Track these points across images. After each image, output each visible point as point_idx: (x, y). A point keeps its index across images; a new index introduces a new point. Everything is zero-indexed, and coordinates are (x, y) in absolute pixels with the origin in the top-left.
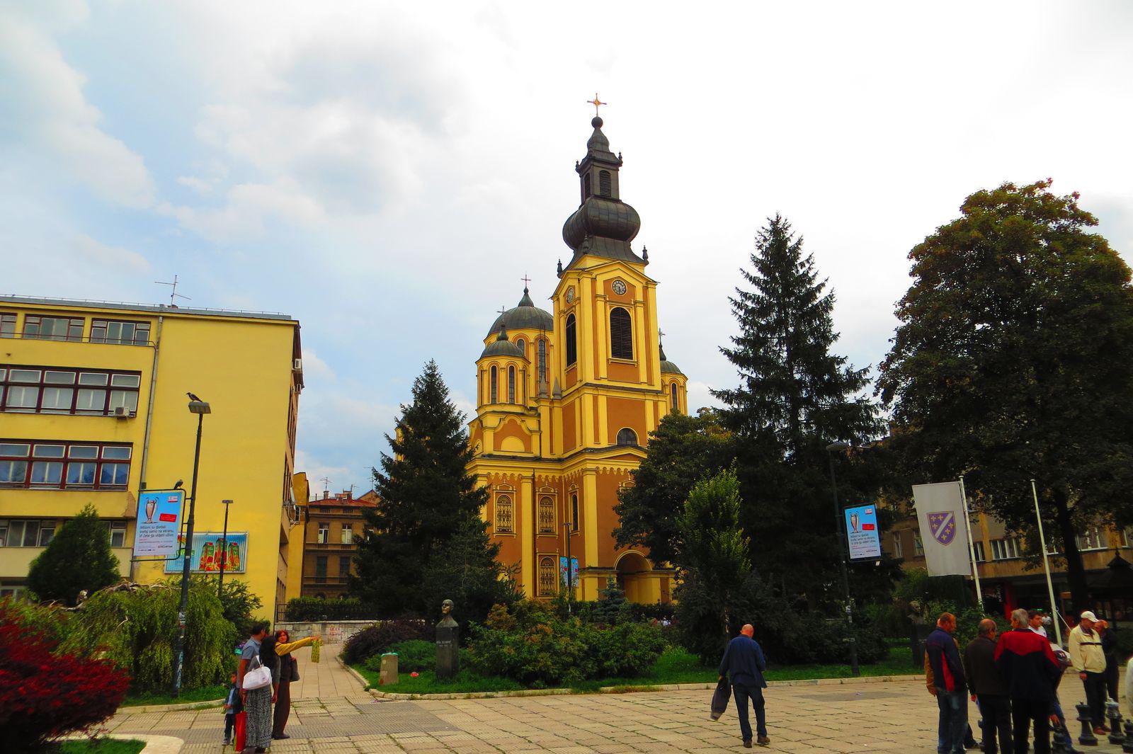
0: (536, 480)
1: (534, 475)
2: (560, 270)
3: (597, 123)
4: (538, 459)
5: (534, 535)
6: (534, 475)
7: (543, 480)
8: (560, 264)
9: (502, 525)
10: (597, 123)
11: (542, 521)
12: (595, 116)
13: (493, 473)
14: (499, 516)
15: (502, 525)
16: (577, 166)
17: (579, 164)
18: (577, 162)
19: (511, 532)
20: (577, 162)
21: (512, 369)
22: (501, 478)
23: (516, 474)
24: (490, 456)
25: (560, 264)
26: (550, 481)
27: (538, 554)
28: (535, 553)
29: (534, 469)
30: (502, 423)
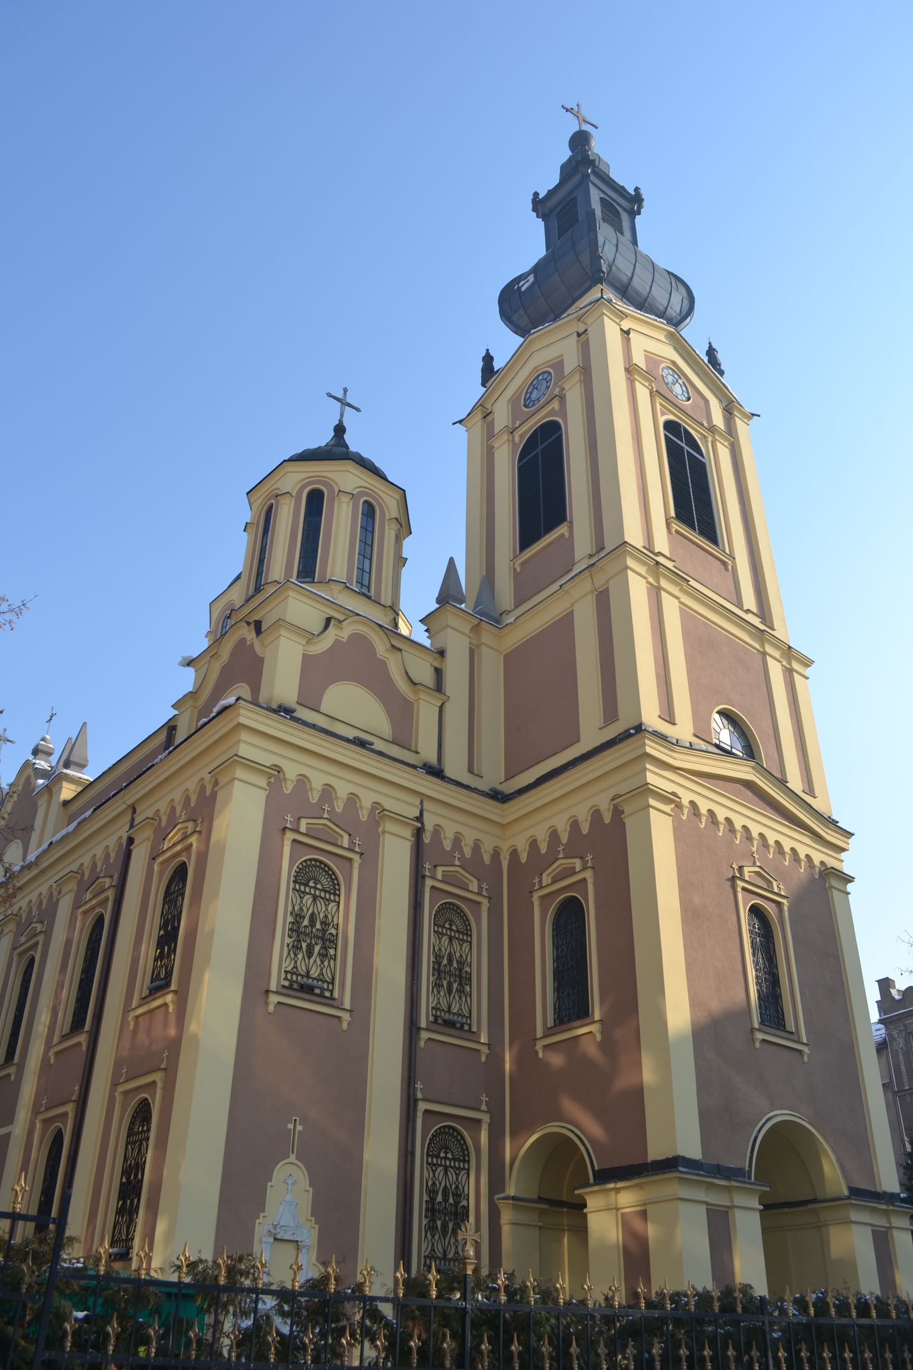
0: (427, 838)
1: (420, 819)
4: (436, 772)
5: (412, 1028)
6: (420, 819)
7: (448, 845)
8: (488, 359)
9: (302, 969)
11: (438, 985)
13: (292, 771)
14: (295, 929)
15: (302, 969)
17: (541, 197)
19: (331, 1001)
20: (536, 194)
21: (369, 511)
22: (314, 797)
23: (367, 799)
24: (284, 711)
25: (488, 359)
26: (468, 852)
27: (422, 1106)
28: (409, 1103)
29: (423, 798)
30: (332, 633)
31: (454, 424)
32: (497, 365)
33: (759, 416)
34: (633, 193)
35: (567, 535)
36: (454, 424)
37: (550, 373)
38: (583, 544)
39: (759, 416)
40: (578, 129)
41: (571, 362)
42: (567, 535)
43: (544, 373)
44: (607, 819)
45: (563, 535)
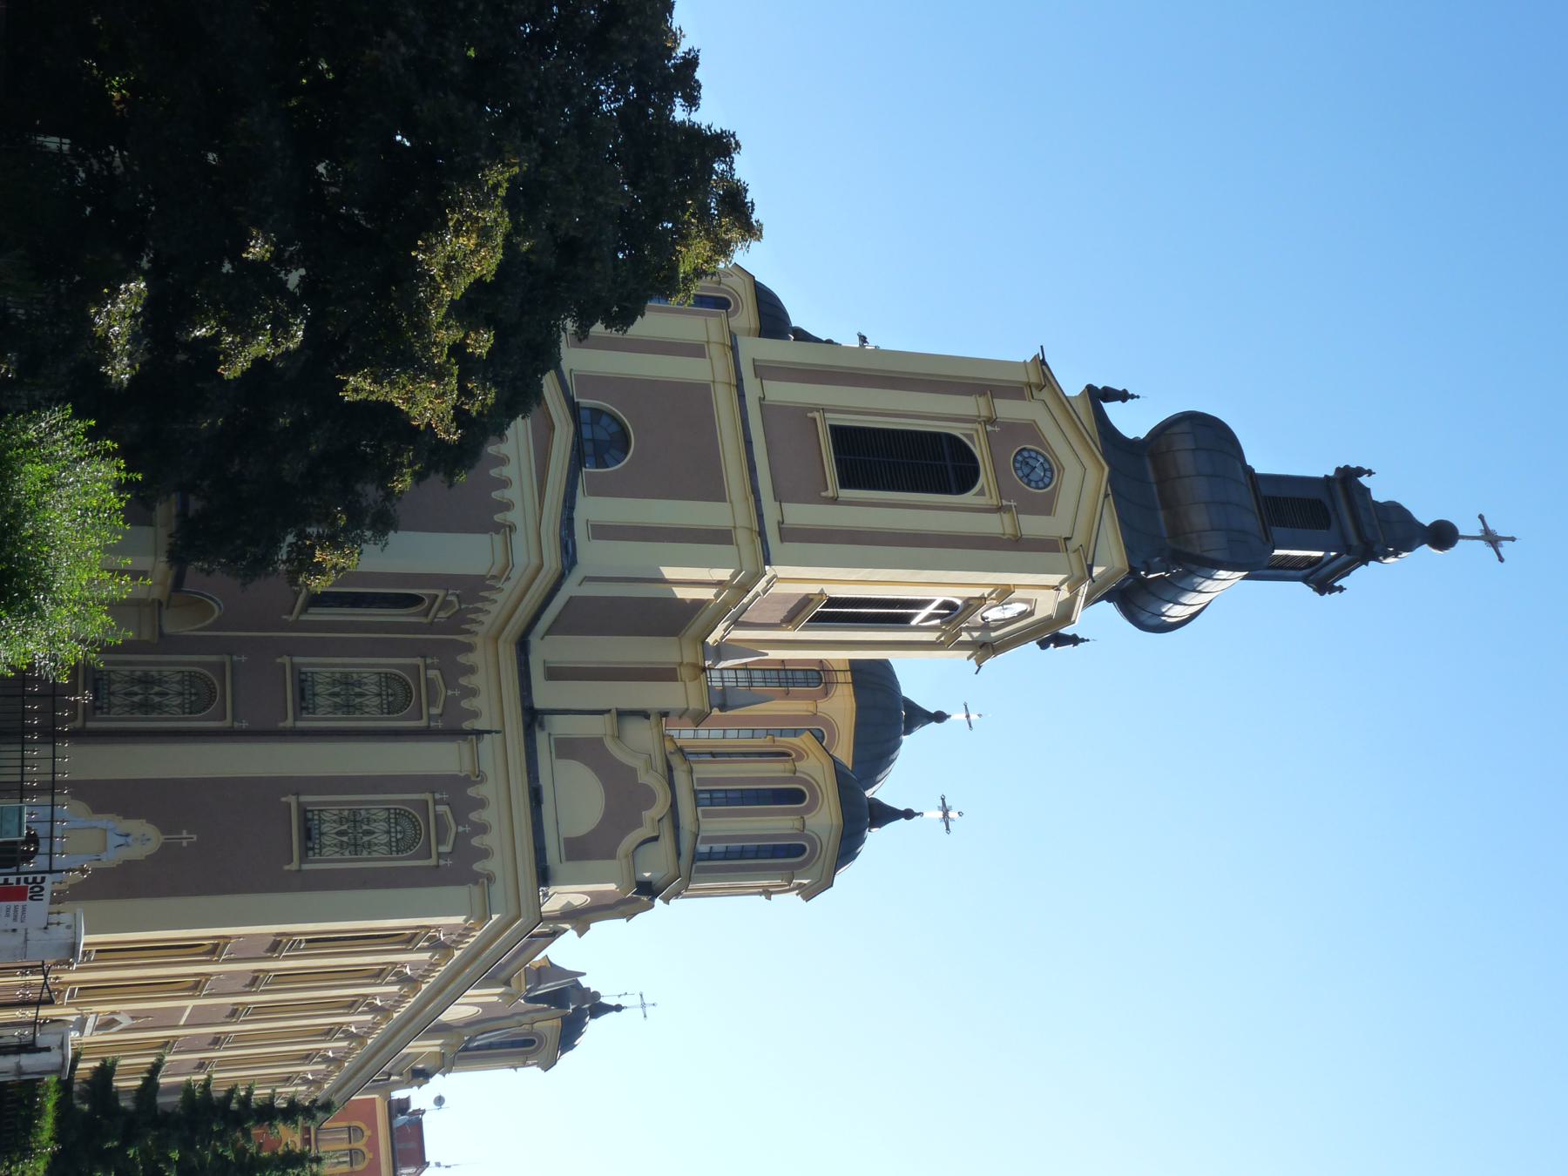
2: (1111, 395)
3: (1443, 535)
8: (1124, 396)
10: (1443, 535)
12: (1461, 533)
16: (1360, 471)
17: (1364, 480)
18: (1370, 473)
20: (1370, 473)
25: (1124, 396)
31: (1042, 347)
32: (1112, 410)
33: (977, 673)
34: (1337, 584)
35: (823, 494)
36: (1042, 347)
37: (1047, 486)
38: (802, 514)
39: (977, 673)
40: (1461, 533)
41: (1033, 525)
42: (823, 494)
43: (1051, 479)
44: (498, 518)
45: (826, 489)
